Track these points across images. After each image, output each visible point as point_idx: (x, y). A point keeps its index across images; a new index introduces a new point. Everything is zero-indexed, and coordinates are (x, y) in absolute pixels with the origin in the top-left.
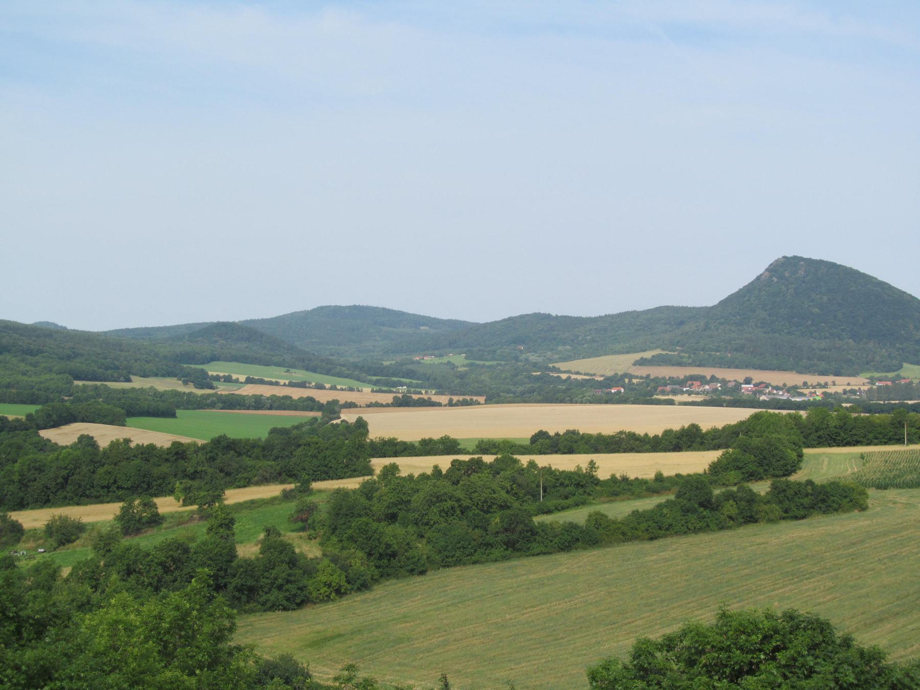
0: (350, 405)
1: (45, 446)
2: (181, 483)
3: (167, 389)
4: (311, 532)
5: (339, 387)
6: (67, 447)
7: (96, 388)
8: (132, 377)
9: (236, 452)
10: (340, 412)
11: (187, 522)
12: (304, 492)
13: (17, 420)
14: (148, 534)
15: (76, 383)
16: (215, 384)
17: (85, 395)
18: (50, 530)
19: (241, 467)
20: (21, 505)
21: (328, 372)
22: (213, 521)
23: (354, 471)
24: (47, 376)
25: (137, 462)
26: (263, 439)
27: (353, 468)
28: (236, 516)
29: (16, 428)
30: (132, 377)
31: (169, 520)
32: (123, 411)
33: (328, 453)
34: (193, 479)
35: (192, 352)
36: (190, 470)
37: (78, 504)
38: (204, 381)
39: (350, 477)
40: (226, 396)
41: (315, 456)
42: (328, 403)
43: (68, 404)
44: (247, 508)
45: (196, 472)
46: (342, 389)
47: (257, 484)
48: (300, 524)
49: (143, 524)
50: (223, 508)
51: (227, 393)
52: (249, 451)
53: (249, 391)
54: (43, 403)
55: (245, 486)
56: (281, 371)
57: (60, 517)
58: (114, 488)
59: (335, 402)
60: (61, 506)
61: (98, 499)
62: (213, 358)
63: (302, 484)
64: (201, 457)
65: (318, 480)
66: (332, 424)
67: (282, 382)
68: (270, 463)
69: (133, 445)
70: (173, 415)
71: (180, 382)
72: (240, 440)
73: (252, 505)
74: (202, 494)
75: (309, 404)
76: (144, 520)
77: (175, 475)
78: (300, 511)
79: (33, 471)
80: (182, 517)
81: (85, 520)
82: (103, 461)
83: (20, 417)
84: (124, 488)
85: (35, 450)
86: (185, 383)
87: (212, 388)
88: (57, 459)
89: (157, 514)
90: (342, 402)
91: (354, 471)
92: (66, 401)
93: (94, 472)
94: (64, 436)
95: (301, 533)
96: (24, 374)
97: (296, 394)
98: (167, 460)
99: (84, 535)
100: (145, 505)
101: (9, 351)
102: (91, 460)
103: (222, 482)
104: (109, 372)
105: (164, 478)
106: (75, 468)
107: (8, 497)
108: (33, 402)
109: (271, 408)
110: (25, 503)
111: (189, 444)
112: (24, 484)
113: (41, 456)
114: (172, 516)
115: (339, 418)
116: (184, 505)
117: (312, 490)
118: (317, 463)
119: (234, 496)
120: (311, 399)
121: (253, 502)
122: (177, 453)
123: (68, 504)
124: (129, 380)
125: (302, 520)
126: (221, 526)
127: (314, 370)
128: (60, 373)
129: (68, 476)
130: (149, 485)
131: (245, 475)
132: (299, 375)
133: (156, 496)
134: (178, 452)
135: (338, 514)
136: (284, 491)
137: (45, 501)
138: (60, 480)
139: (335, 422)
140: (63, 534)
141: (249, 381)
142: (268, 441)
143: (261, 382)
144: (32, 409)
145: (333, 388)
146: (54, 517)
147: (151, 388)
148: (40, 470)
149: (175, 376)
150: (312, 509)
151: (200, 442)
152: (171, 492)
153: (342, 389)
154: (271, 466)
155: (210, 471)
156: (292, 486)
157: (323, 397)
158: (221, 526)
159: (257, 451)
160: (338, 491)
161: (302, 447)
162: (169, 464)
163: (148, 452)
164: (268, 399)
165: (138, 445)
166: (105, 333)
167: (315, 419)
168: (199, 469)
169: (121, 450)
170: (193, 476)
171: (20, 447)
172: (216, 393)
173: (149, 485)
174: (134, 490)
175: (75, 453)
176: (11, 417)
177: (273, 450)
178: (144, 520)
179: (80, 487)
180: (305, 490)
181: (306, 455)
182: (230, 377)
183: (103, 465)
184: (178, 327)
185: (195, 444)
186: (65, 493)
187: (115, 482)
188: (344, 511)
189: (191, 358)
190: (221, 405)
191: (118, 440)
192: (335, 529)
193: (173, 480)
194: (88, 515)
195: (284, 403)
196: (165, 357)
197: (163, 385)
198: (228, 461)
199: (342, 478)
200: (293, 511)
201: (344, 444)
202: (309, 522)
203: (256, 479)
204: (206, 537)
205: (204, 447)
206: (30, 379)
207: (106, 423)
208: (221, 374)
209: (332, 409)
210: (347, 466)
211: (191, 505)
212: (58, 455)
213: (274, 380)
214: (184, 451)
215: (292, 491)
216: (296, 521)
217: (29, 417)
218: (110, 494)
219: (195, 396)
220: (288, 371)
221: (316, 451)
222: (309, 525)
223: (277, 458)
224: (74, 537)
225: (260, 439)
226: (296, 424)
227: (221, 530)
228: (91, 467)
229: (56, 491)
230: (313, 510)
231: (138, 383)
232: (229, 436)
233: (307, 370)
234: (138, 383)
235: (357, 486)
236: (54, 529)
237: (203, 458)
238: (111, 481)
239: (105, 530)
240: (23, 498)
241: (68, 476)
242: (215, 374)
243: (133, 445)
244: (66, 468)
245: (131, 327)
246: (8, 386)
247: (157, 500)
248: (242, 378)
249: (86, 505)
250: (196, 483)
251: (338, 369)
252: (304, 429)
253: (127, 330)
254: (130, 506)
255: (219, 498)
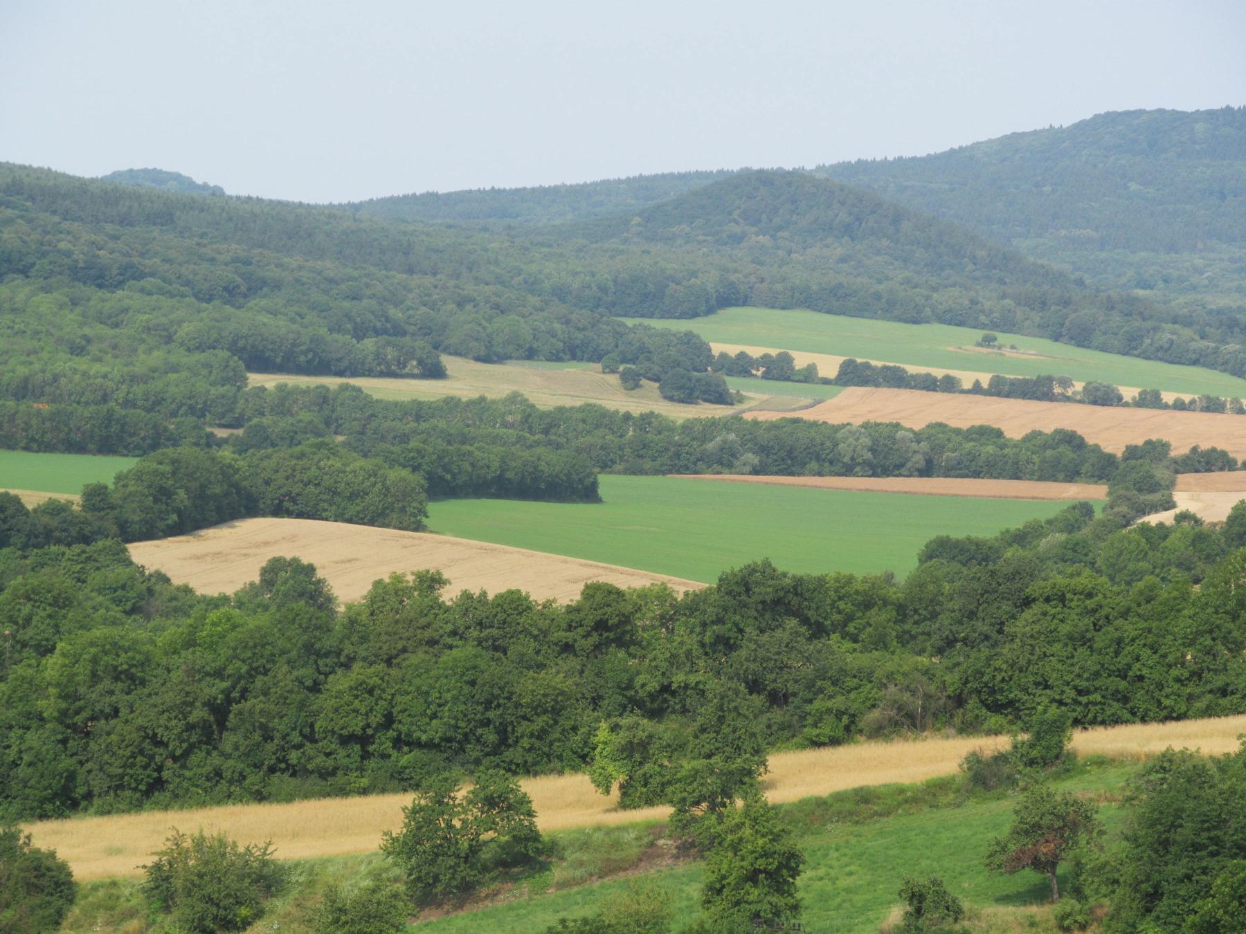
0: (1209, 462)
1: (146, 597)
2: (615, 728)
3: (568, 402)
4: (1069, 904)
5: (1168, 397)
6: (224, 599)
7: (323, 398)
8: (447, 361)
9: (805, 621)
10: (1172, 485)
11: (635, 864)
12: (1045, 762)
13: (55, 509)
14: (502, 901)
15: (256, 380)
16: (733, 384)
17: (285, 423)
18: (163, 886)
19: (822, 674)
20: (66, 800)
21: (1131, 346)
22: (730, 865)
23: (1224, 692)
24: (157, 357)
25: (464, 652)
26: (901, 578)
27: (1219, 681)
28: (804, 844)
29: (48, 536)
30: (447, 361)
31: (571, 856)
32: (416, 479)
33: (1130, 628)
34: (656, 714)
35: (647, 275)
36: (648, 683)
37: (260, 797)
38: (694, 376)
39: (1208, 712)
40: (773, 426)
41: (1082, 640)
42: (1132, 452)
43: (226, 454)
44: (842, 816)
45: (665, 689)
46: (1180, 406)
47: (878, 732)
48: (1030, 876)
49: (485, 869)
50: (760, 817)
51: (774, 416)
52: (850, 618)
53: (851, 409)
54: (142, 451)
55: (835, 742)
56: (966, 339)
57: (199, 843)
58: (383, 742)
59: (1155, 450)
60: (203, 804)
61: (329, 782)
62: (730, 298)
63: (1038, 737)
64: (685, 637)
65: (1094, 722)
66: (1145, 530)
67: (967, 379)
68: (923, 660)
69: (448, 595)
70: (589, 494)
71: (614, 379)
72: (821, 581)
73: (862, 804)
74: (687, 765)
75: (1065, 457)
76: (486, 855)
77: (596, 701)
78: (1030, 830)
79: (107, 683)
80: (616, 845)
81: (284, 852)
82: (348, 649)
83: (62, 497)
84: (419, 745)
85: (116, 611)
86: (631, 382)
87: (721, 398)
88: (190, 643)
89: (534, 836)
90: (1179, 449)
91: (1224, 692)
92: (221, 443)
93: (315, 688)
94: (215, 564)
95: (1034, 910)
96: (77, 350)
97: (1018, 420)
98: (567, 648)
99: (281, 905)
100: (491, 802)
101: (25, 272)
102: (308, 648)
103: (758, 727)
104: (369, 344)
105: (556, 711)
106: (253, 673)
107: (22, 771)
108: (107, 447)
109: (927, 471)
110: (81, 790)
111: (643, 595)
112: (75, 726)
113: (136, 631)
114: (584, 841)
115: (1169, 505)
116: (624, 805)
117: (1072, 756)
118: (1092, 663)
119: (798, 776)
120: (1071, 440)
121: (864, 797)
122: (601, 626)
123: (229, 797)
124: (435, 372)
125: (1037, 864)
126: (752, 877)
127: (1082, 337)
128: (200, 348)
129: (229, 701)
130: (503, 732)
131: (839, 702)
132: (1029, 354)
133: (529, 770)
134: (606, 623)
135: (1165, 844)
136: (974, 760)
137: (147, 788)
138: (198, 714)
139: (1153, 519)
140: (209, 900)
141: (853, 375)
142: (917, 584)
143: (896, 379)
144: (105, 470)
145: (1150, 400)
146: (177, 840)
147: (514, 398)
148: (131, 678)
149: (596, 357)
150: (1071, 823)
151: (682, 587)
152: (583, 758)
153: (1180, 406)
154: (928, 673)
155: (714, 686)
156: (1003, 743)
157: (1111, 432)
158: (752, 877)
159: (879, 617)
160: (1165, 764)
161: (1036, 608)
162: (573, 663)
163: (502, 621)
164: (918, 437)
165: (466, 596)
166: (356, 207)
167: (1085, 509)
168: (678, 678)
169: (409, 614)
170: (658, 704)
171: (61, 602)
172: (737, 418)
173: (503, 732)
174: (452, 748)
175: (252, 623)
176: (32, 499)
177: (934, 616)
178: (486, 855)
179: (267, 738)
180: (1048, 756)
181: (1051, 637)
182: (785, 359)
183: (347, 666)
184: (606, 188)
185: (663, 595)
186: (215, 760)
187: (389, 721)
188: (1186, 833)
189: (650, 296)
190: (753, 458)
191: (397, 579)
192: (1155, 895)
193: (588, 716)
194: (295, 835)
195: (980, 456)
196: (560, 293)
197: (553, 388)
198: (776, 652)
199: (1179, 718)
200: (1006, 830)
201: (1185, 596)
202: (1063, 868)
203: (875, 714)
204: (700, 915)
205: (693, 605)
206: (96, 368)
207: (361, 521)
208: (755, 352)
209: (1144, 473)
210: (1197, 675)
211: (650, 802)
212: (194, 627)
213: (939, 373)
214: (626, 619)
215: (1001, 758)
216: (1015, 864)
217: (96, 496)
218: (372, 763)
219: (665, 427)
220: (988, 341)
221: (1087, 621)
222: (1062, 881)
223: (950, 642)
224: (244, 911)
225: (889, 578)
226: (1016, 525)
227: (754, 894)
228: (307, 673)
229: (187, 753)
230: (1074, 827)
231: (466, 381)
232: (781, 567)
233: (1057, 338)
234: (466, 381)
235: (1233, 747)
236: (178, 883)
237: (692, 642)
238: (375, 719)
239: (352, 888)
240: (72, 776)
241: (229, 701)
242: (733, 350)
243: (448, 595)
244: (219, 674)
245: (443, 188)
246: (23, 390)
247: (531, 787)
248: (829, 367)
249: (289, 799)
250: (667, 729)
251: (1164, 337)
252: (1043, 544)
253: (431, 200)
254: (441, 803)
255: (743, 779)
